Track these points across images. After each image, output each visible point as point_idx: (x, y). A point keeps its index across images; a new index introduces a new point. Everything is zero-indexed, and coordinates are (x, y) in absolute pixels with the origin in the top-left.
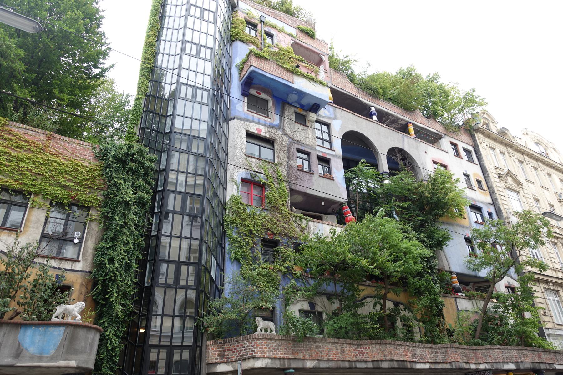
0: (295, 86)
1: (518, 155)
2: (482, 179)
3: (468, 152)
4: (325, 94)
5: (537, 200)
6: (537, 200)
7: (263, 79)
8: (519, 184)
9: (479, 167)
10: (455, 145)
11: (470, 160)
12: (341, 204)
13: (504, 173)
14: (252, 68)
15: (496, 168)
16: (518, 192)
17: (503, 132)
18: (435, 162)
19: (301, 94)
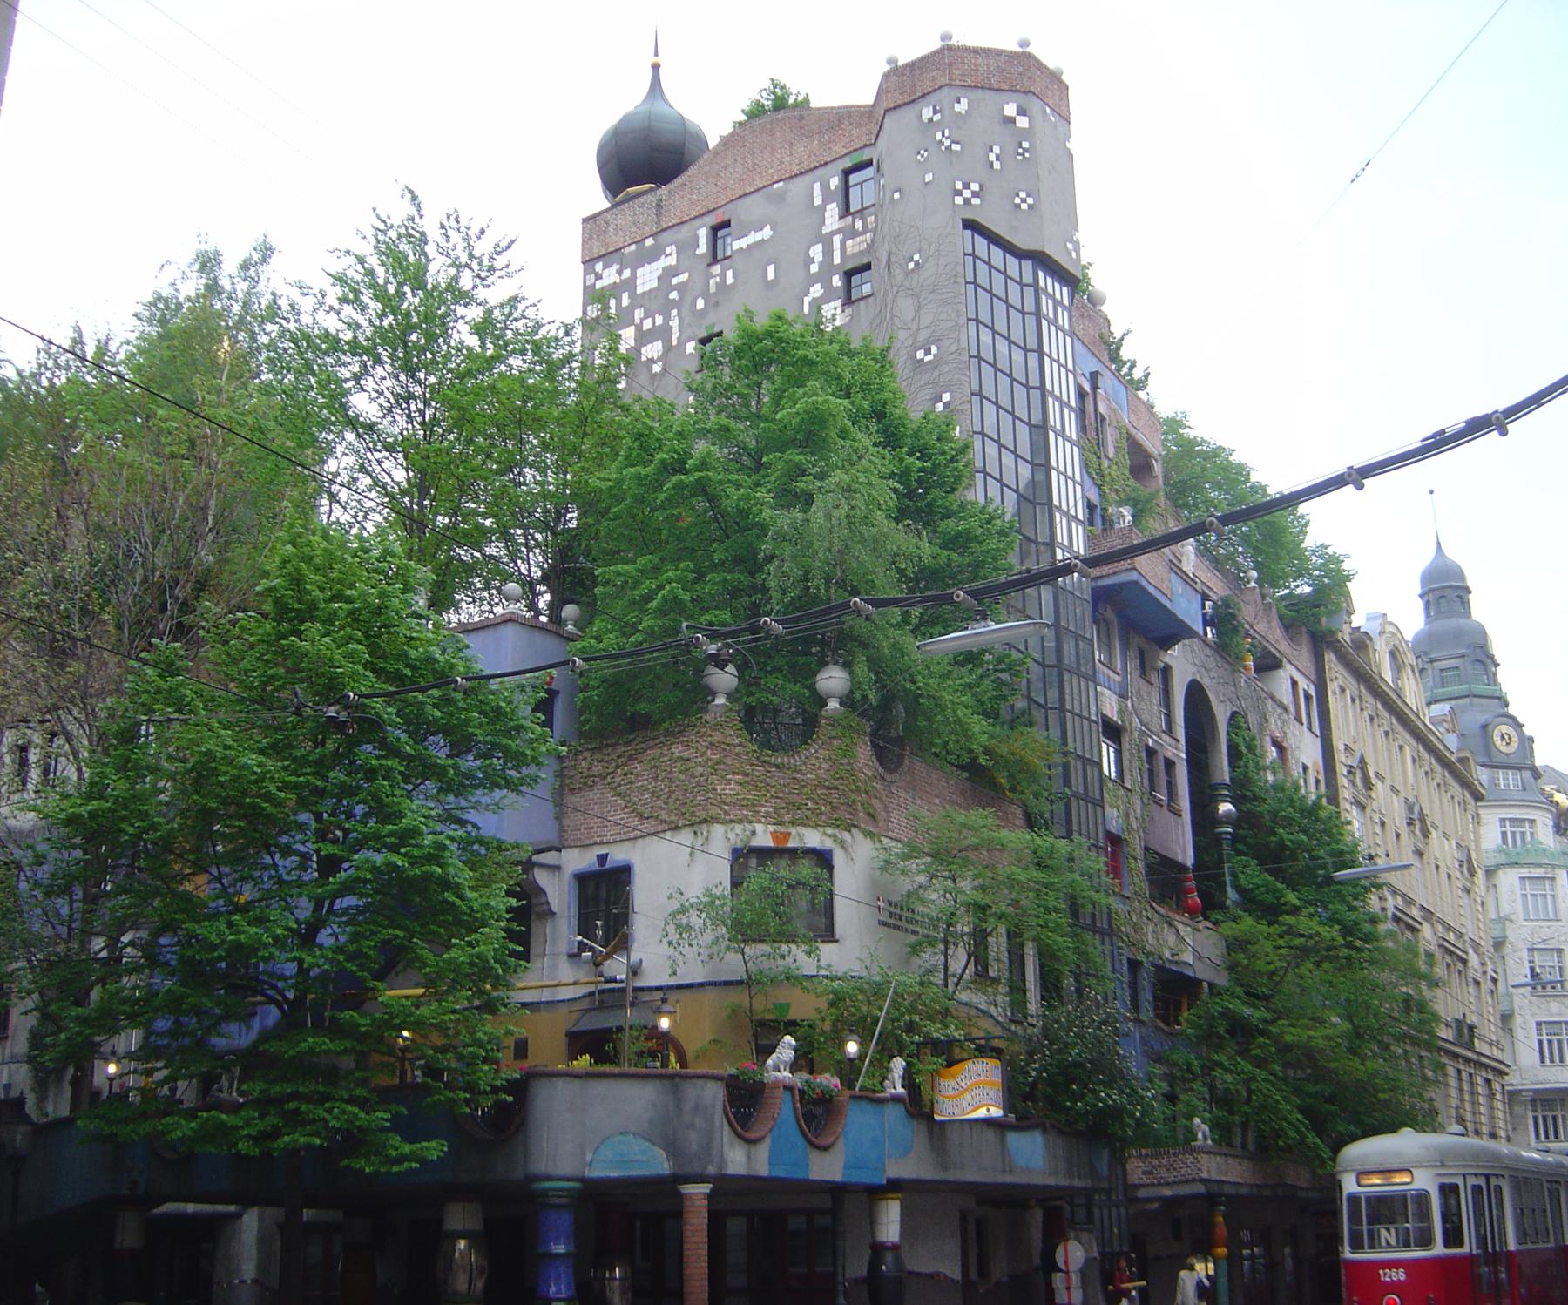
1: (1369, 698)
2: (1322, 778)
3: (1308, 697)
5: (1383, 824)
6: (1383, 824)
8: (1368, 786)
9: (1318, 742)
10: (1294, 683)
12: (1182, 868)
14: (1134, 576)
15: (1347, 748)
16: (1362, 807)
17: (1362, 641)
18: (1275, 743)
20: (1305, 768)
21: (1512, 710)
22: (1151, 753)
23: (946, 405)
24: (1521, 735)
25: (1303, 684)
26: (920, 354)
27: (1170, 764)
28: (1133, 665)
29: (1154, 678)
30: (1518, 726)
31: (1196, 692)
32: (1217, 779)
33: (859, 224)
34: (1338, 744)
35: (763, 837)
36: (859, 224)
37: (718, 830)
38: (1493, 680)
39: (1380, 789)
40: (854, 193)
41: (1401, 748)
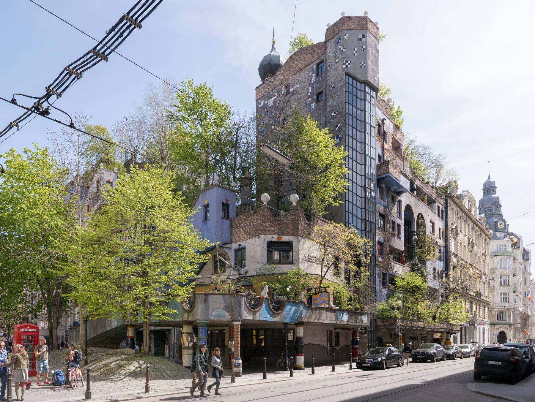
0: (401, 183)
1: (460, 212)
2: (444, 231)
3: (442, 211)
4: (405, 183)
7: (390, 179)
10: (439, 207)
11: (442, 218)
13: (454, 227)
17: (460, 197)
18: (431, 222)
19: (401, 187)
20: (439, 229)
21: (504, 218)
22: (393, 222)
23: (339, 128)
24: (505, 224)
25: (441, 207)
26: (333, 114)
27: (399, 226)
28: (390, 200)
29: (397, 203)
30: (504, 221)
31: (408, 207)
32: (412, 230)
33: (320, 79)
34: (450, 222)
35: (275, 238)
36: (320, 79)
37: (263, 236)
38: (500, 210)
39: (461, 235)
40: (320, 70)
41: (469, 225)
